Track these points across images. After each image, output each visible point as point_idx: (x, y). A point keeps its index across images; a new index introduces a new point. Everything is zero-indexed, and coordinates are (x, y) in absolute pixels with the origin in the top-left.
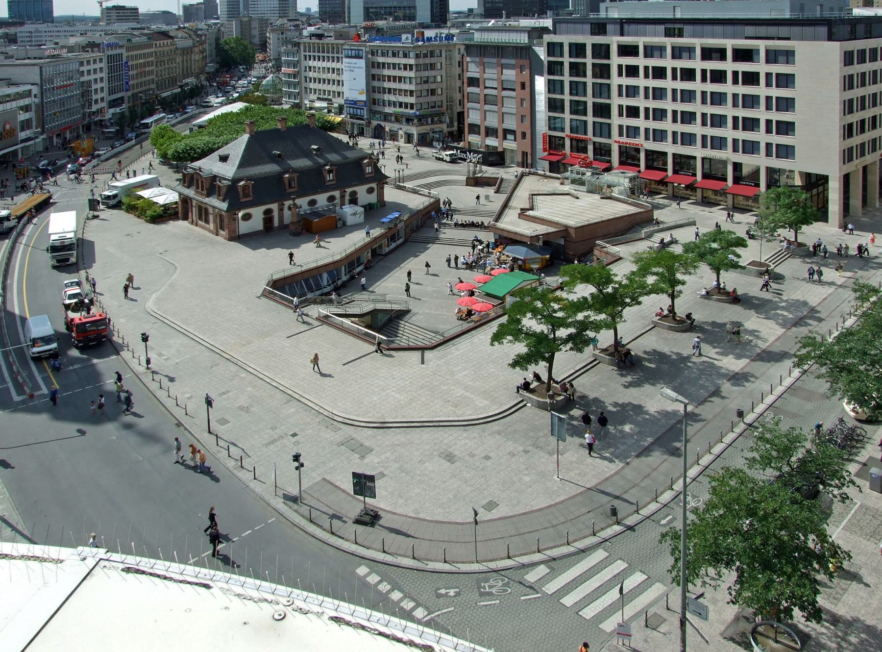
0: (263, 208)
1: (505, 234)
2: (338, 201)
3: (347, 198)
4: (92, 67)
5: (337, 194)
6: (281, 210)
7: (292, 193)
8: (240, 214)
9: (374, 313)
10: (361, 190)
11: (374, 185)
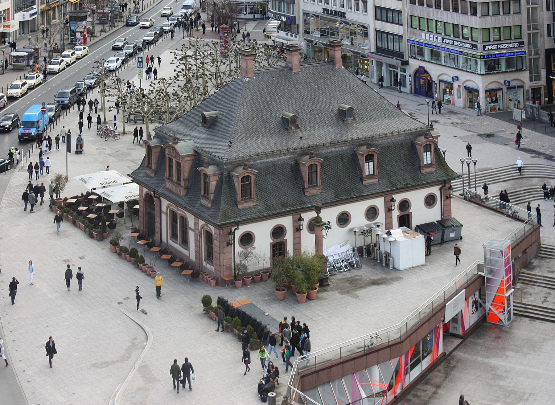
2: (381, 218)
3: (396, 213)
5: (379, 203)
6: (297, 230)
8: (238, 234)
10: (416, 198)
11: (435, 190)
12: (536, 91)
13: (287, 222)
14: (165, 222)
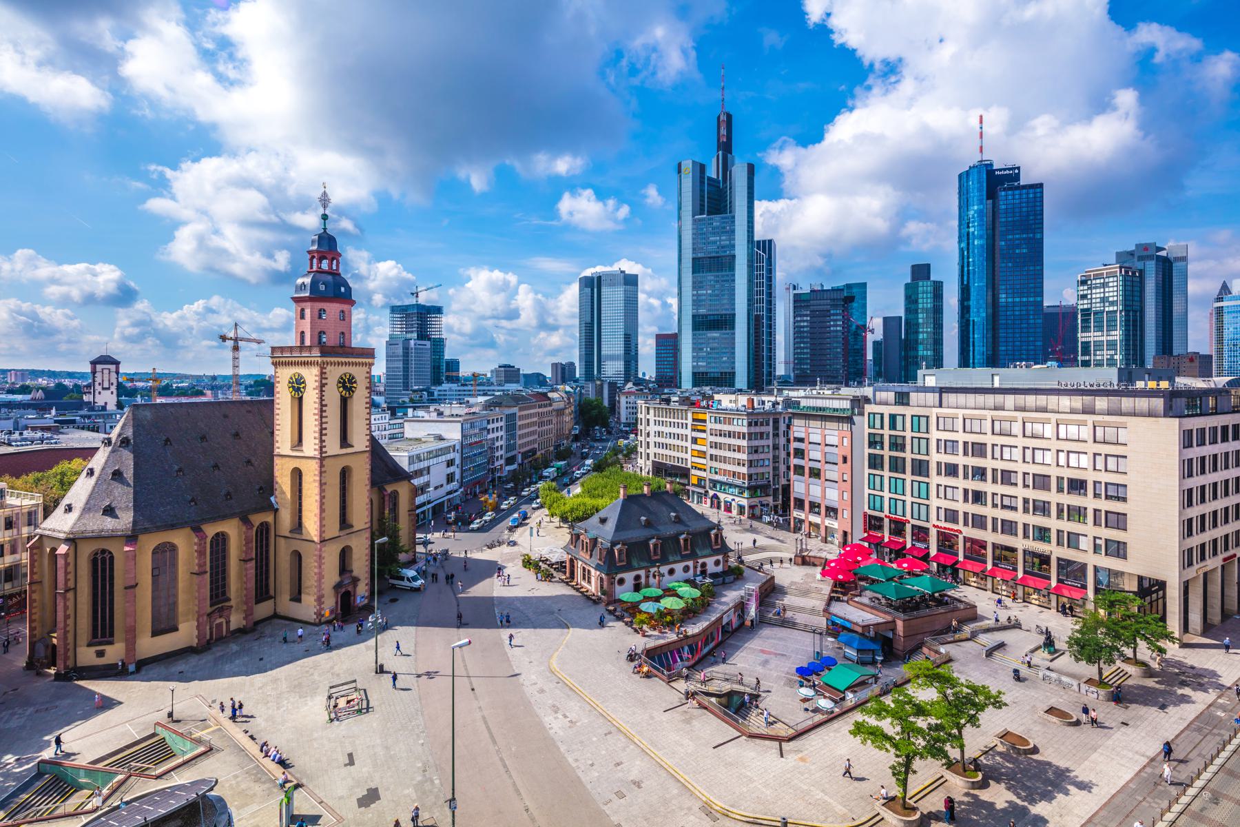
0: (634, 573)
1: (838, 621)
3: (699, 569)
4: (496, 425)
5: (690, 563)
6: (647, 577)
7: (657, 561)
9: (731, 694)
11: (720, 557)
12: (776, 506)
13: (642, 573)
14: (579, 573)
